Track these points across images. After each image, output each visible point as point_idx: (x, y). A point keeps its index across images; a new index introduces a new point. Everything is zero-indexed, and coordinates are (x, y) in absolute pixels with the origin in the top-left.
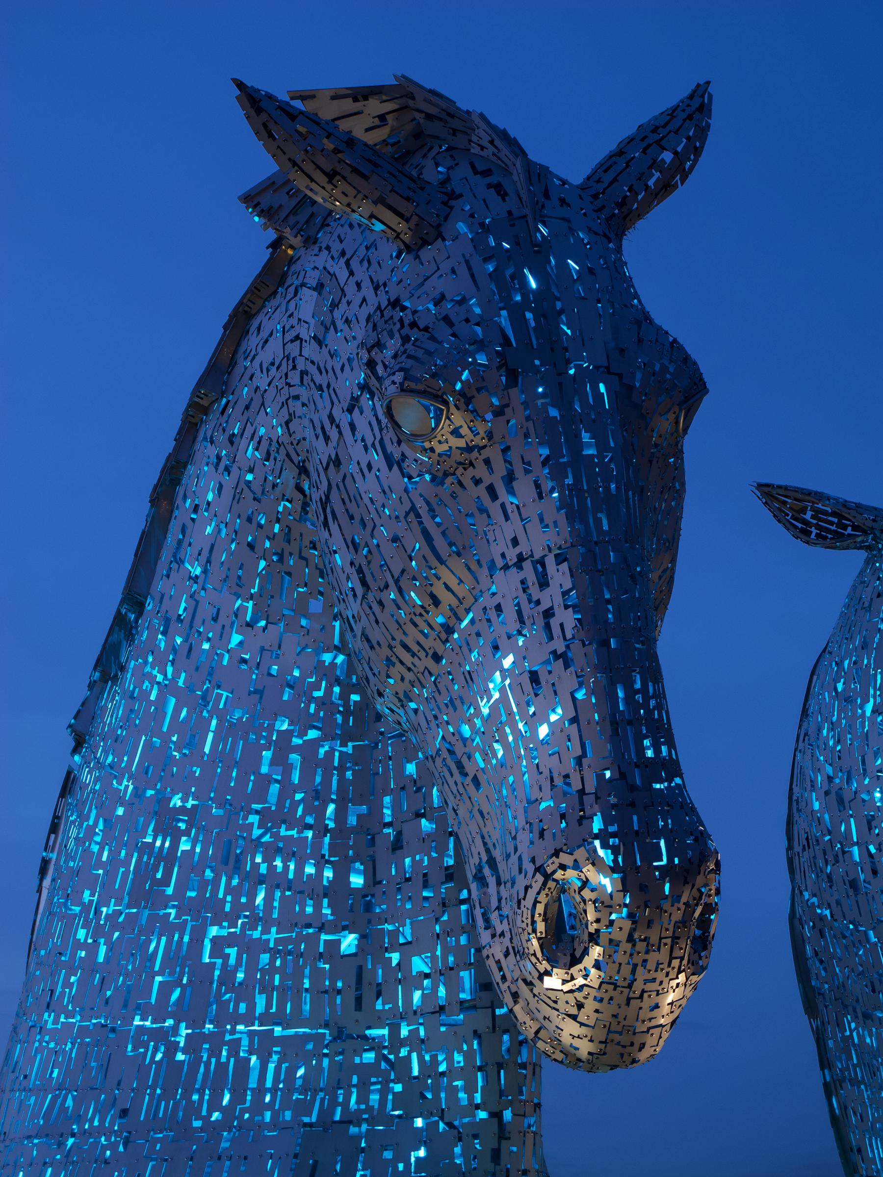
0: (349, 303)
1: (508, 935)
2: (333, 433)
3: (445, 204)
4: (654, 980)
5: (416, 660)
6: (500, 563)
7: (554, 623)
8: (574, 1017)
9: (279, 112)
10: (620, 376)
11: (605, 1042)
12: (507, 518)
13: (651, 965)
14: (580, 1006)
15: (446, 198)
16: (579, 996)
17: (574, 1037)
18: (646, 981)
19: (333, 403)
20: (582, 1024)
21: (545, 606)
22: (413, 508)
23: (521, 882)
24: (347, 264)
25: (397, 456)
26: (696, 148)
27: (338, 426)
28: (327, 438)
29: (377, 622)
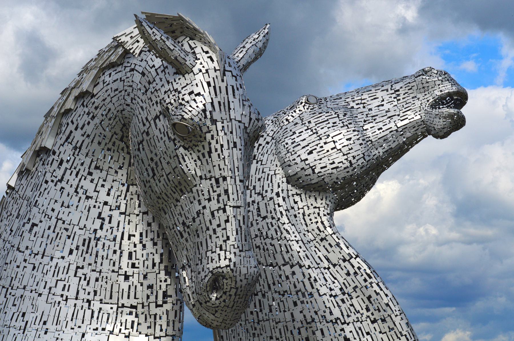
0: (157, 84)
1: (194, 288)
2: (147, 124)
3: (194, 61)
4: (239, 306)
5: (169, 199)
6: (204, 177)
7: (221, 199)
8: (214, 315)
9: (147, 26)
10: (244, 124)
11: (221, 323)
12: (208, 164)
13: (239, 302)
14: (216, 311)
15: (194, 59)
16: (217, 309)
17: (212, 320)
18: (237, 306)
19: (148, 115)
20: (216, 317)
21: (218, 192)
22: (177, 156)
23: (203, 274)
24: (156, 70)
25: (173, 137)
26: (265, 46)
27: (149, 122)
28: (144, 125)
29: (157, 185)
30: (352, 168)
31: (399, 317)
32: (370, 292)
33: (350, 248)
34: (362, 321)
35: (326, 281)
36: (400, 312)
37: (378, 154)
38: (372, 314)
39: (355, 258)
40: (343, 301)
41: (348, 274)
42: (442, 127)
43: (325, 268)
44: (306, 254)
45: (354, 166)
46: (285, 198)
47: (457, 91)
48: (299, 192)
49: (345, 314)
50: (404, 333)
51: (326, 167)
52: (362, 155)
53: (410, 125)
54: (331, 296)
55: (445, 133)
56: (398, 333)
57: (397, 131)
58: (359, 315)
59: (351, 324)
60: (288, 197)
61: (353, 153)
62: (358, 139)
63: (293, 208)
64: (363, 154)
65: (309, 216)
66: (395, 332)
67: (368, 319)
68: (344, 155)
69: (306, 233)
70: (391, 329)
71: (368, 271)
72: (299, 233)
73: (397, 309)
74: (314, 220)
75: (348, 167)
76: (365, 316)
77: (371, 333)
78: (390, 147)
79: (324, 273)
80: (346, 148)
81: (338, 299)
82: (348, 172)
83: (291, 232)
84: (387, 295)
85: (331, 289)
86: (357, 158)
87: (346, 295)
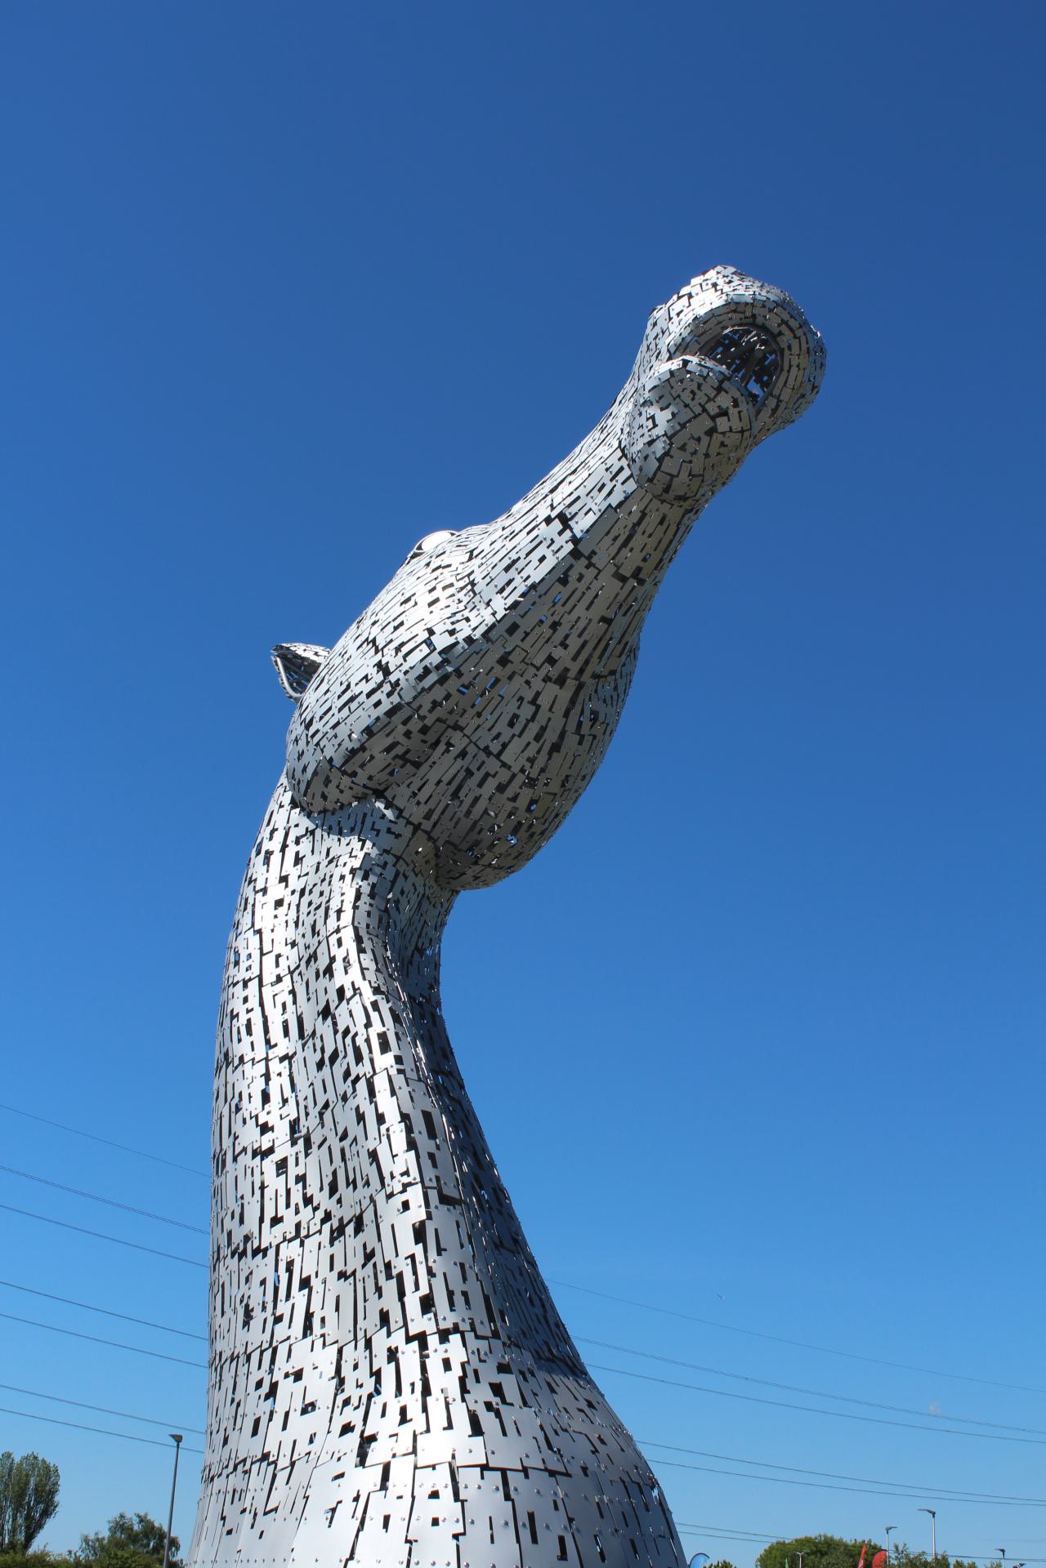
30: (387, 688)
31: (398, 1201)
32: (347, 1119)
33: (355, 970)
34: (307, 1236)
35: (266, 1097)
36: (406, 1179)
37: (490, 620)
38: (339, 1201)
39: (348, 1001)
40: (282, 1166)
41: (320, 1065)
42: (647, 439)
43: (282, 1060)
44: (249, 1021)
45: (393, 678)
46: (272, 853)
47: (727, 304)
48: (312, 826)
49: (269, 1214)
50: (401, 1265)
51: (330, 709)
52: (426, 635)
53: (590, 485)
54: (255, 1154)
55: (660, 460)
56: (381, 1267)
57: (548, 520)
58: (306, 1213)
59: (271, 1253)
60: (284, 847)
61: (402, 635)
62: (434, 589)
63: (284, 879)
64: (431, 632)
65: (311, 892)
66: (375, 1265)
67: (327, 1227)
68: (377, 651)
69: (286, 951)
70: (369, 1256)
71: (360, 1041)
72: (262, 954)
73: (398, 1168)
74: (313, 906)
75: (380, 686)
76: (320, 1214)
77: (314, 1282)
78: (529, 582)
79: (273, 1076)
80: (390, 628)
81: (269, 1165)
82: (377, 704)
83: (243, 957)
84: (381, 1119)
85: (265, 1129)
86: (405, 650)
87: (301, 1142)
